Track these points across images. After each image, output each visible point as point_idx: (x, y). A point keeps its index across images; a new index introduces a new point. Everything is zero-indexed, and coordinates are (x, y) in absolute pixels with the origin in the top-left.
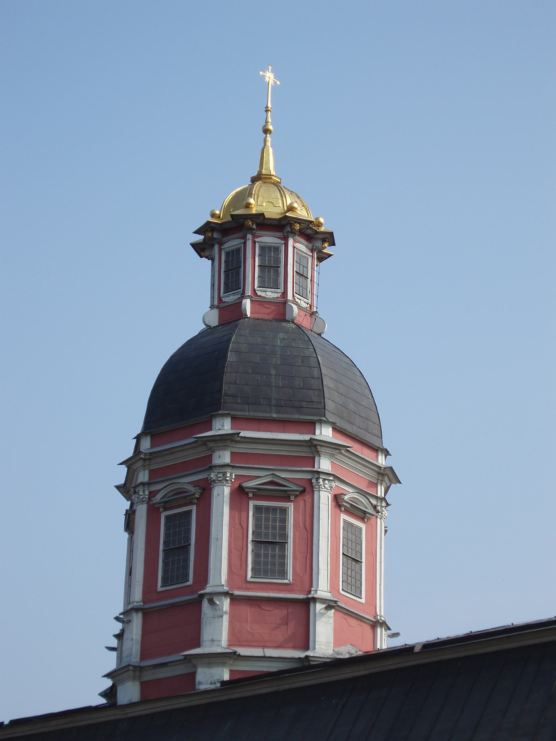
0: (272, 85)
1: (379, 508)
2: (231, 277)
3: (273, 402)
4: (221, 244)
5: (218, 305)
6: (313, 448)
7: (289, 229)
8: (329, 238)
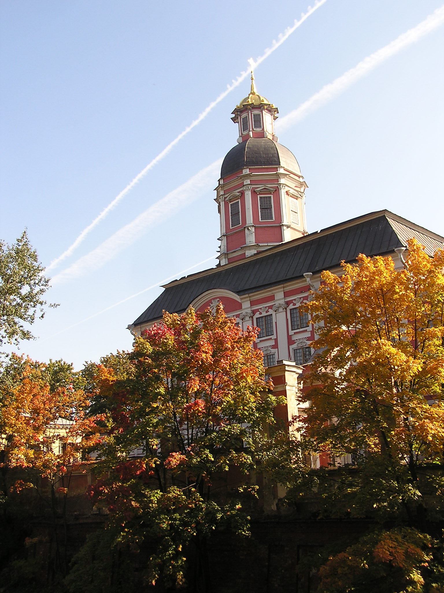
2: (245, 126)
4: (240, 116)
5: (242, 136)
8: (276, 110)
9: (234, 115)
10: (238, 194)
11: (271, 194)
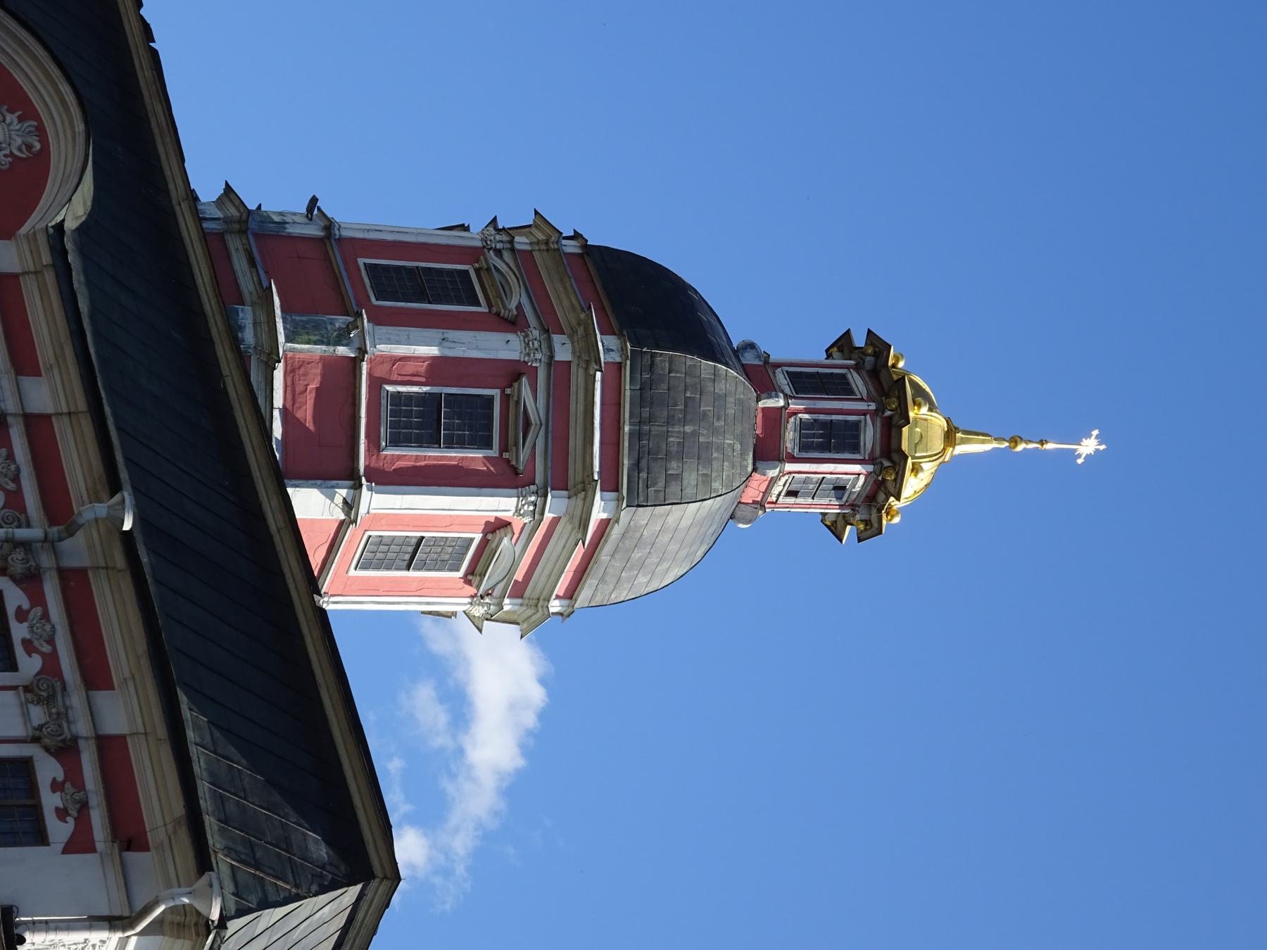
0: (1075, 450)
1: (487, 600)
3: (646, 428)
4: (857, 368)
6: (580, 486)
7: (886, 464)
8: (871, 530)
9: (859, 341)
10: (513, 305)
11: (504, 448)
